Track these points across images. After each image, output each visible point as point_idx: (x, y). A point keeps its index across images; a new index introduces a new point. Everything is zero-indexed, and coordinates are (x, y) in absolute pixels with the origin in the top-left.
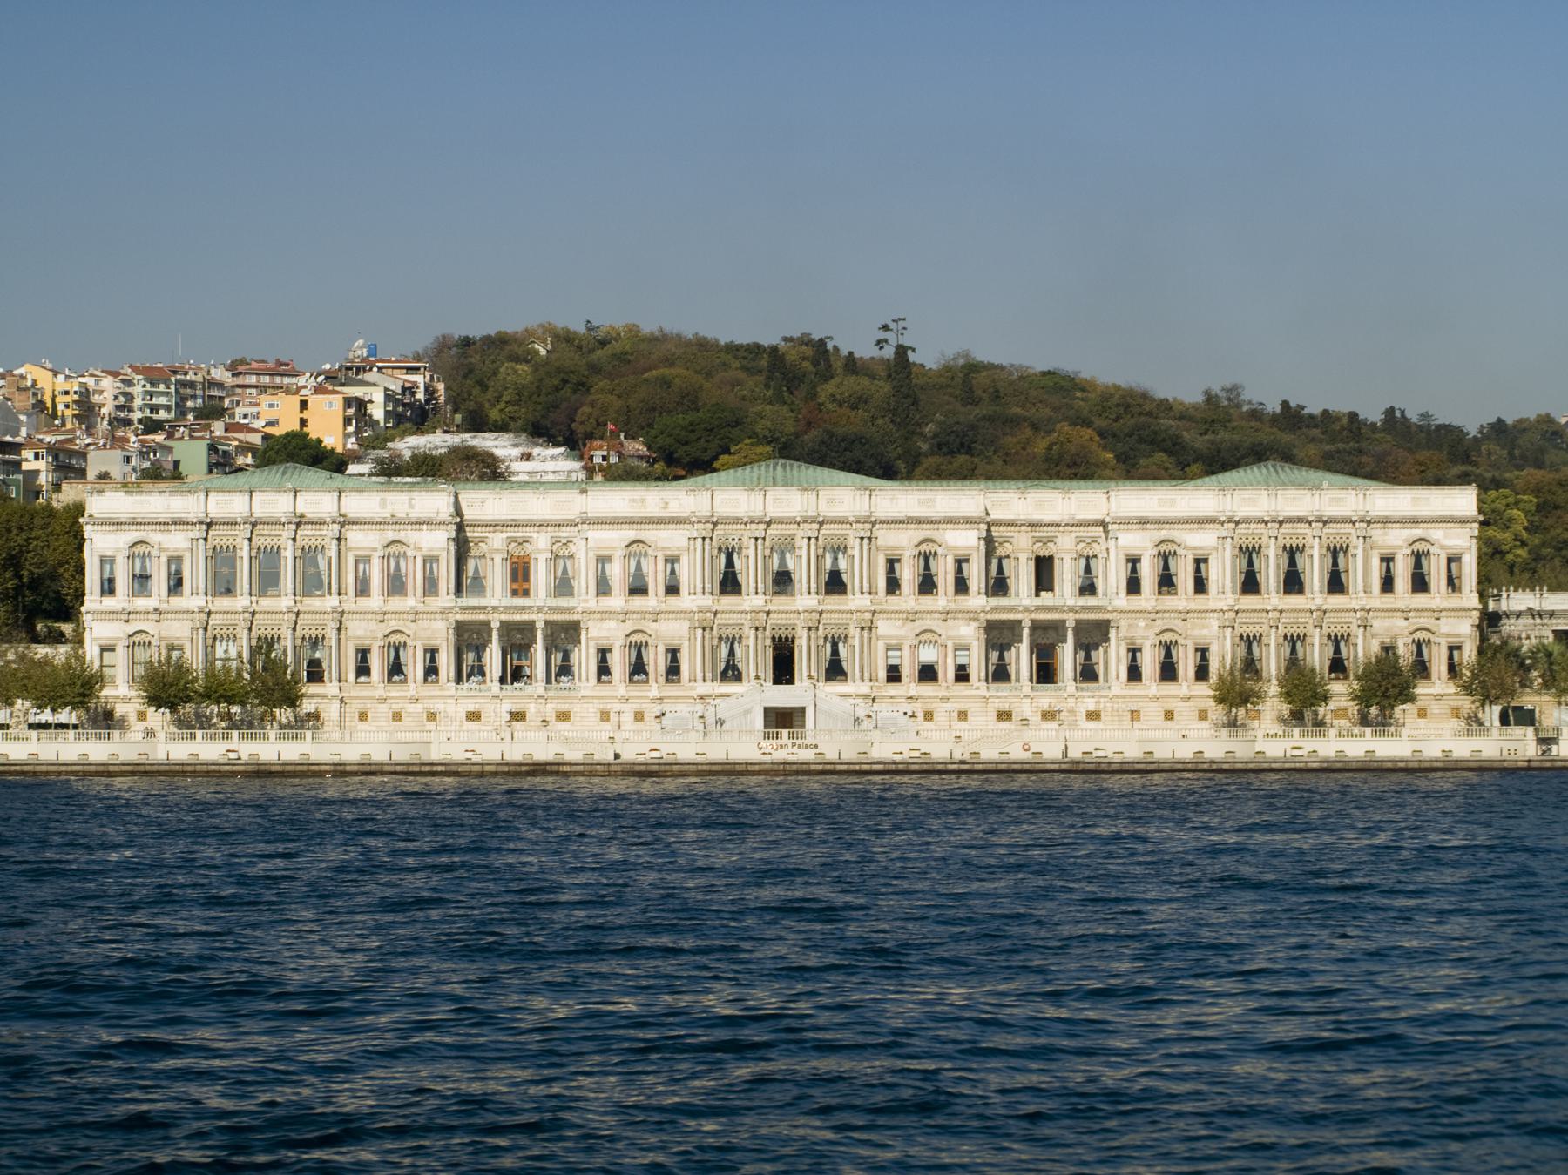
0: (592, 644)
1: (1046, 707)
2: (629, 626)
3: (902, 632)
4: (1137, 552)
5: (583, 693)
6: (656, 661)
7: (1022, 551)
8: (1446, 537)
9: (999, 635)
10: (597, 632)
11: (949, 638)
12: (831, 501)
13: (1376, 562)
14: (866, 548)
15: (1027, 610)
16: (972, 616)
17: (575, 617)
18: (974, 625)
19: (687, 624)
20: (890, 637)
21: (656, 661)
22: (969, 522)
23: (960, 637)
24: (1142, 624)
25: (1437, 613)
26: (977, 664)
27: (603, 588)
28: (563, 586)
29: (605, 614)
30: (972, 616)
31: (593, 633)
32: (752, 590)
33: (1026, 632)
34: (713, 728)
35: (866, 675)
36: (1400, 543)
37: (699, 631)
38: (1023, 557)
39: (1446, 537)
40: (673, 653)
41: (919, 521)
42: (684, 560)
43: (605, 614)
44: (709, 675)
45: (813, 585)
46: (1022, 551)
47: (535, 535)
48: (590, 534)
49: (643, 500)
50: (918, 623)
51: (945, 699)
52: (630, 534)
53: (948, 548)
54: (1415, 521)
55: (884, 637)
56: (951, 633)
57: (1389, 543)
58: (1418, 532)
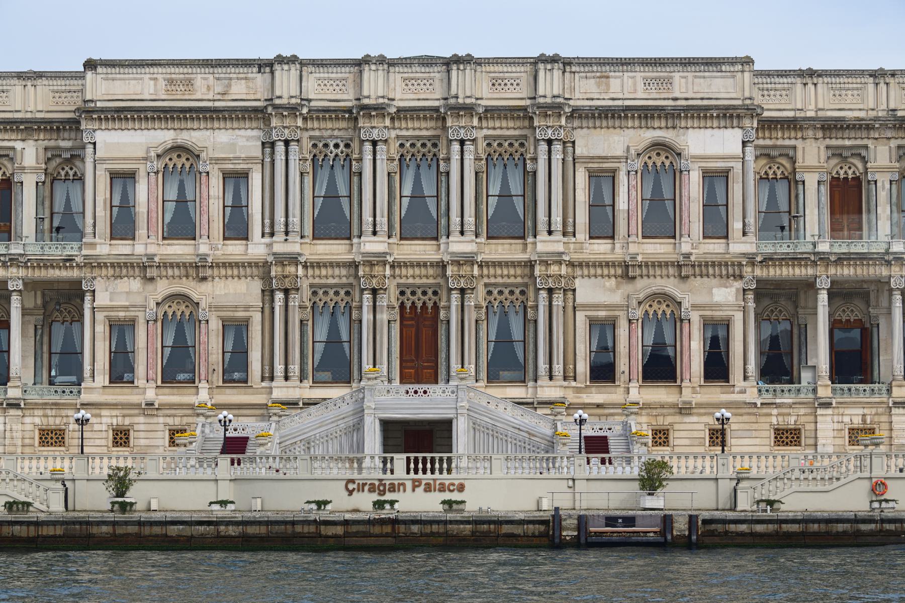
0: (100, 316)
1: (857, 421)
2: (163, 288)
3: (617, 298)
5: (85, 397)
6: (212, 346)
7: (810, 169)
9: (778, 300)
10: (110, 296)
11: (695, 307)
12: (494, 83)
14: (557, 156)
15: (823, 259)
16: (728, 269)
17: (75, 274)
18: (739, 284)
19: (257, 286)
20: (596, 307)
21: (212, 346)
22: (728, 115)
26: (744, 352)
27: (123, 225)
28: (64, 225)
29: (122, 267)
30: (728, 269)
31: (102, 299)
32: (368, 228)
33: (823, 297)
34: (315, 458)
35: (558, 368)
37: (279, 296)
38: (811, 180)
40: (236, 330)
41: (647, 114)
42: (256, 180)
43: (122, 267)
44: (295, 368)
45: (470, 219)
46: (810, 169)
47: (19, 145)
48: (101, 137)
49: (189, 83)
50: (640, 283)
51: (684, 410)
52: (163, 136)
55: (586, 307)
56: (700, 299)
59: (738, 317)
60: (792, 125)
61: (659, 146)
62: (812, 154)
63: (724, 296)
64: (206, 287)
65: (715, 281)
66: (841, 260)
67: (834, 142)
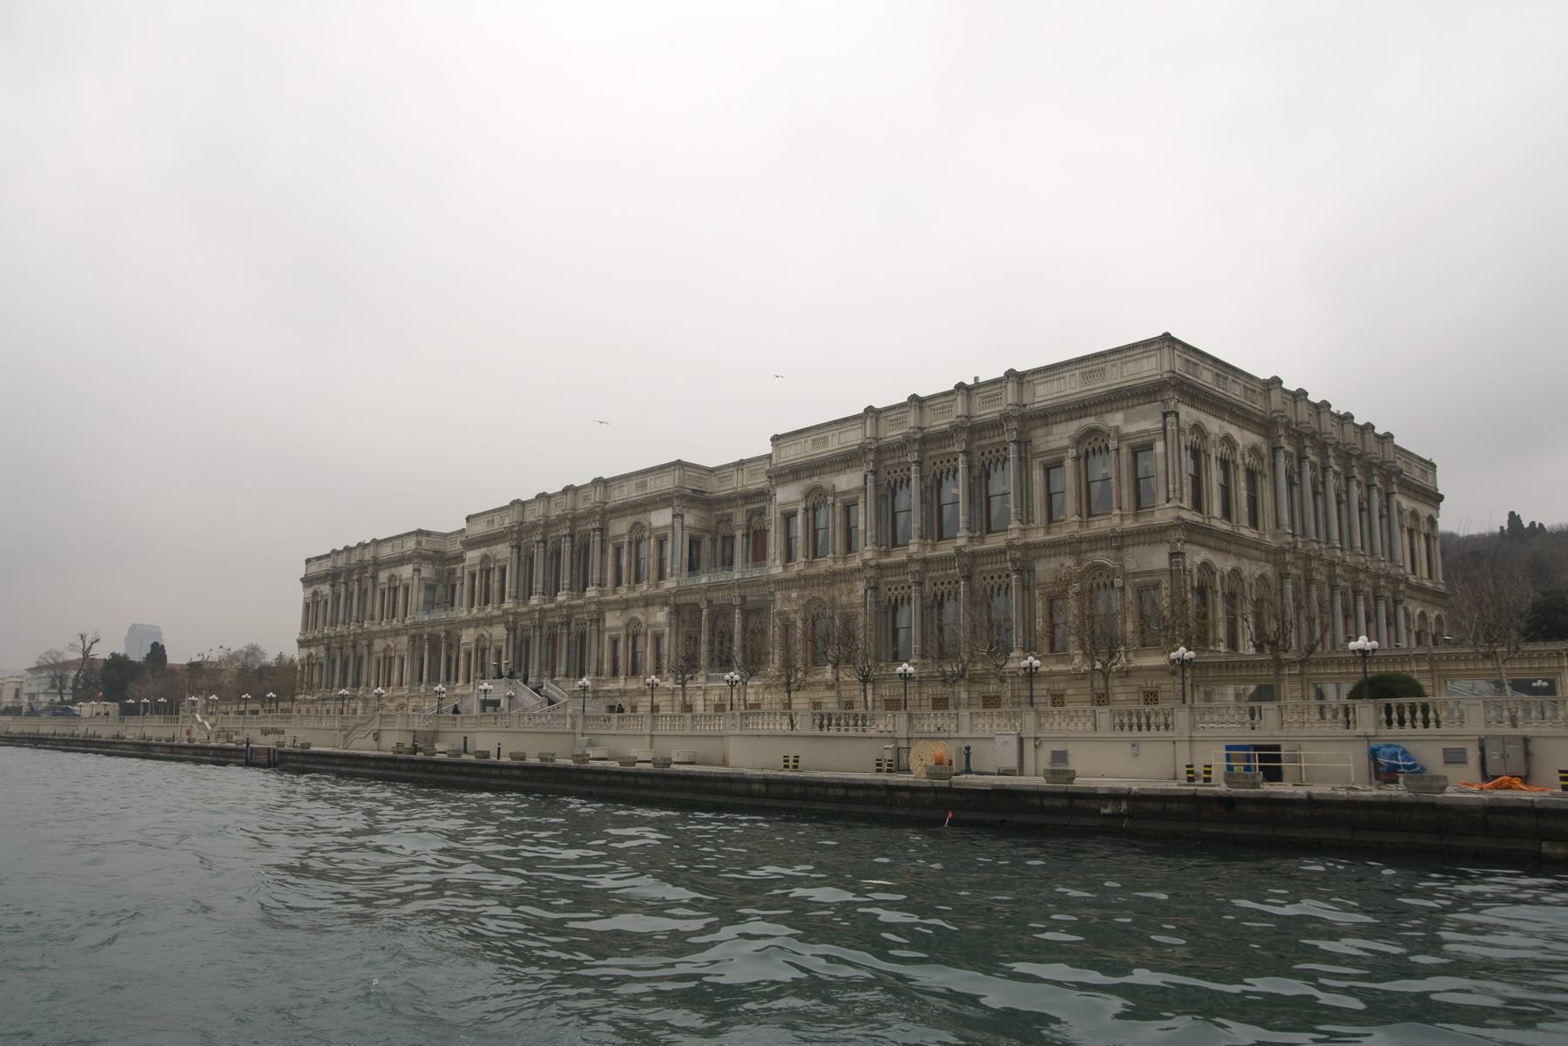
4: (792, 507)
7: (738, 527)
8: (1127, 420)
13: (1037, 475)
18: (667, 609)
20: (612, 629)
23: (655, 625)
24: (794, 595)
25: (1119, 541)
36: (1066, 442)
38: (739, 534)
39: (1127, 420)
43: (468, 624)
46: (738, 527)
53: (651, 530)
54: (1079, 408)
56: (651, 621)
57: (1053, 445)
58: (1090, 421)
59: (667, 630)
60: (729, 500)
61: (637, 523)
62: (739, 517)
63: (661, 616)
64: (490, 630)
65: (657, 608)
66: (710, 587)
67: (751, 507)
